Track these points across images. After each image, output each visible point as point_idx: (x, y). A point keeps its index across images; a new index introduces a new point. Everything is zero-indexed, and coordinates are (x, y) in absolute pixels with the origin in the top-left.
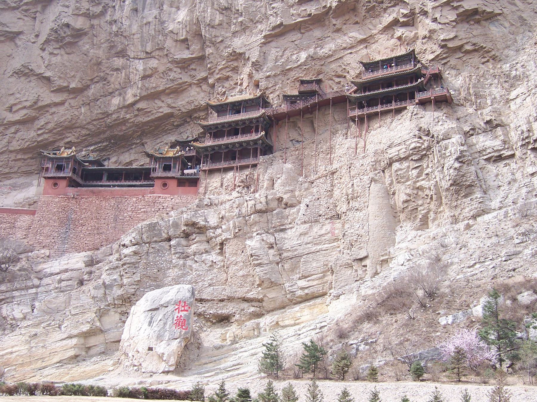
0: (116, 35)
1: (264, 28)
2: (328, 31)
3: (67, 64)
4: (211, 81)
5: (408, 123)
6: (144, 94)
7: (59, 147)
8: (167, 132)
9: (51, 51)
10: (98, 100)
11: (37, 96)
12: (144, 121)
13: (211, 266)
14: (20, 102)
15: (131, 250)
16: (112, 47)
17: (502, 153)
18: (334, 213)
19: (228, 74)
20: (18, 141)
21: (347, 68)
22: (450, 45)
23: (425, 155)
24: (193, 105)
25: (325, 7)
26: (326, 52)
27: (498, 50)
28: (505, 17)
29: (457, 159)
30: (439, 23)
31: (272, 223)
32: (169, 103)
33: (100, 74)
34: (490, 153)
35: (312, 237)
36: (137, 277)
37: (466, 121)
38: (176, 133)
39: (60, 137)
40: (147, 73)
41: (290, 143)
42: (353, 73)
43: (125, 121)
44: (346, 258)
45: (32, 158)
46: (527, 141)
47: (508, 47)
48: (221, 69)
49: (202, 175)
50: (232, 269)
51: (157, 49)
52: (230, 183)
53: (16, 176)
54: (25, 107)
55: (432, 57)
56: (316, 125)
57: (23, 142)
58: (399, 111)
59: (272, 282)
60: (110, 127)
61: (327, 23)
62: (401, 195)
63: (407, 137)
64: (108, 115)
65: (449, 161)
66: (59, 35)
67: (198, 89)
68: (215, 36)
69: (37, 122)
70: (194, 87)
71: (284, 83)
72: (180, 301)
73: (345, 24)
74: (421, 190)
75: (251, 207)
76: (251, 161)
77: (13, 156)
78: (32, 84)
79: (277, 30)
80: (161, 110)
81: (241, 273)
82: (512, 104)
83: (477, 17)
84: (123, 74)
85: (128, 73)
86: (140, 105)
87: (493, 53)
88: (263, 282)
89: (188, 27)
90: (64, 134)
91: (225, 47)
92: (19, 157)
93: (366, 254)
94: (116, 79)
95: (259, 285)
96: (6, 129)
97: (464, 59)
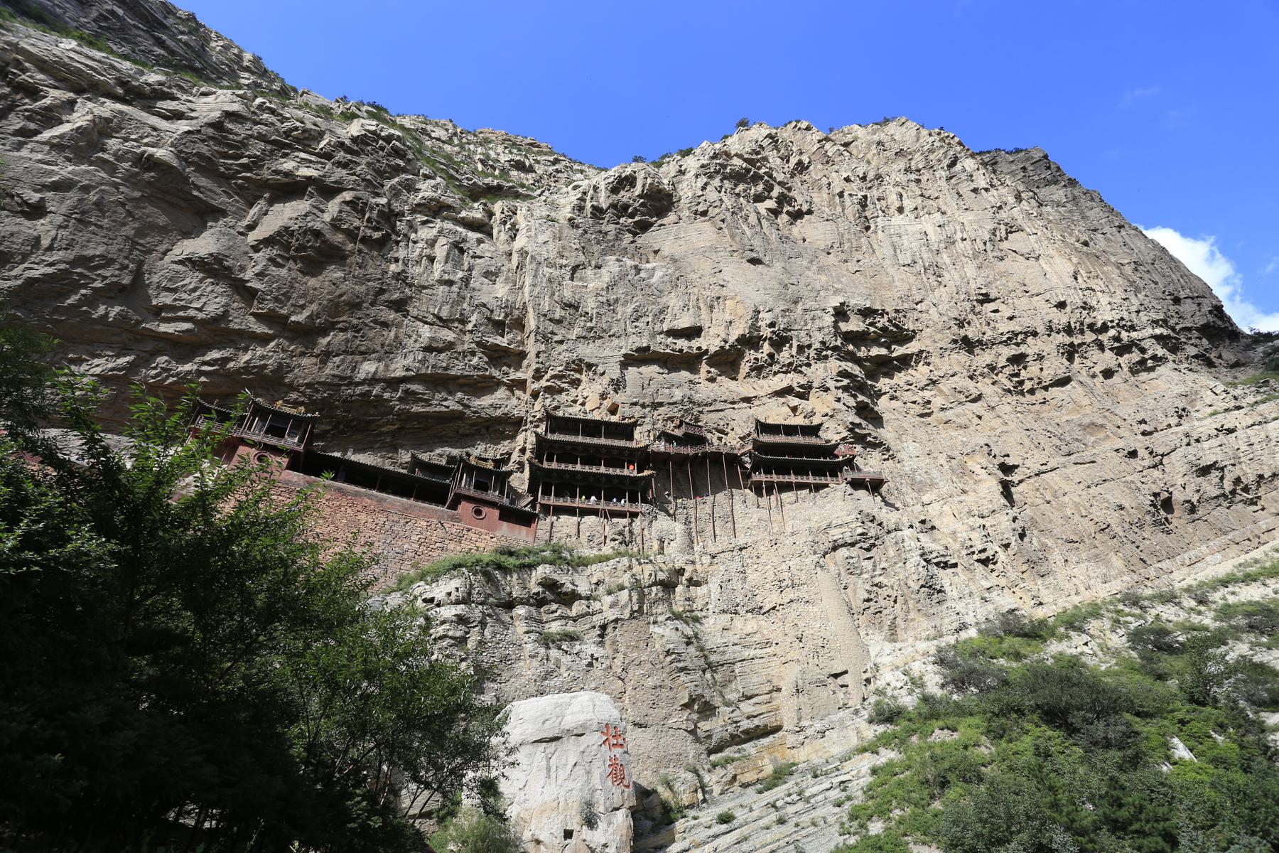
1: (629, 345)
5: (841, 503)
10: (338, 355)
13: (590, 665)
14: (185, 308)
15: (454, 612)
17: (947, 559)
19: (563, 385)
20: (155, 368)
21: (732, 423)
22: (857, 430)
25: (699, 348)
35: (738, 636)
40: (434, 345)
42: (741, 432)
44: (815, 673)
46: (972, 550)
48: (553, 377)
50: (634, 674)
52: (594, 533)
55: (838, 437)
56: (698, 483)
63: (848, 519)
64: (352, 383)
67: (508, 392)
68: (553, 333)
72: (607, 725)
74: (880, 587)
75: (651, 575)
78: (219, 289)
81: (650, 682)
84: (392, 334)
87: (891, 452)
95: (685, 706)
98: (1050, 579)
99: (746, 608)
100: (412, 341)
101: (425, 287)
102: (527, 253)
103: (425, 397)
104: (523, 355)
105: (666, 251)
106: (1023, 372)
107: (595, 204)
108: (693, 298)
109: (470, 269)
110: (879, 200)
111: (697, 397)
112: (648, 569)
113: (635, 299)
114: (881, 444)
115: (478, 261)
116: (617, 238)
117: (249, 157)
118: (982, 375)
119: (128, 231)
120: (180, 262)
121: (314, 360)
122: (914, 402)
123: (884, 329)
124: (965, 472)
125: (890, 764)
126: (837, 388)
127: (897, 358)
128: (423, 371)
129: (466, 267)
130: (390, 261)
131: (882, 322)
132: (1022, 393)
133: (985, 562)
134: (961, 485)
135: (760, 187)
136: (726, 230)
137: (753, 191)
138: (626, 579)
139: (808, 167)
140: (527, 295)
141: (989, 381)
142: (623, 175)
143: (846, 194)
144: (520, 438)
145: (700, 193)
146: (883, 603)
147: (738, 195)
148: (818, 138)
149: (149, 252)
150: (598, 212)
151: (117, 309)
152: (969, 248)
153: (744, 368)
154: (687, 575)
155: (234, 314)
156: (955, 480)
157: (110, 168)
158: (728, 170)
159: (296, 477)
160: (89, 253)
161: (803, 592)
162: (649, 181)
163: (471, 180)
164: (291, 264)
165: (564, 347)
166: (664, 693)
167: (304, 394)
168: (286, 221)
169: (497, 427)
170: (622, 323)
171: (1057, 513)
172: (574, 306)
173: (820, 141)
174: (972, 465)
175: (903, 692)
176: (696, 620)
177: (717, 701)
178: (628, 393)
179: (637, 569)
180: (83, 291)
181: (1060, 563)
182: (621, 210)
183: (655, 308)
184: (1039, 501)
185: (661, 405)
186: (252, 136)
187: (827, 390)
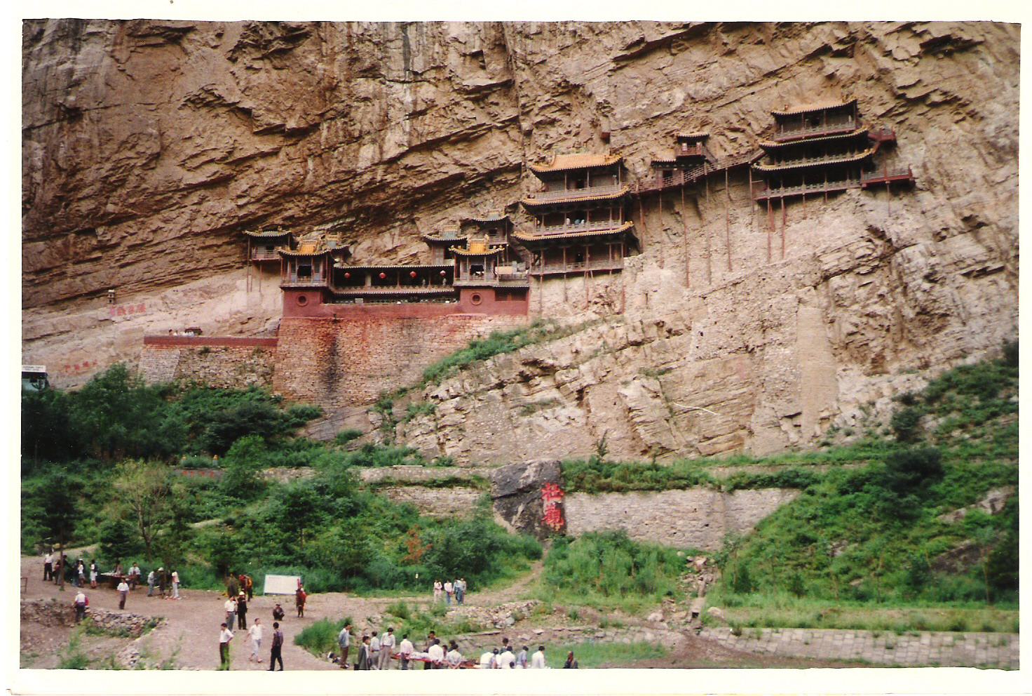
0: (361, 41)
2: (714, 52)
3: (279, 87)
4: (526, 125)
5: (850, 216)
6: (416, 142)
7: (272, 224)
8: (453, 203)
9: (249, 65)
10: (336, 149)
11: (232, 142)
12: (416, 186)
14: (203, 152)
16: (354, 61)
18: (741, 344)
21: (748, 117)
22: (911, 94)
23: (877, 267)
24: (496, 163)
26: (714, 89)
27: (979, 101)
28: (988, 48)
29: (928, 278)
30: (895, 59)
31: (653, 361)
32: (457, 157)
33: (336, 105)
34: (969, 266)
37: (935, 217)
38: (467, 204)
39: (275, 209)
40: (419, 109)
41: (664, 233)
42: (756, 127)
43: (383, 186)
45: (228, 243)
47: (992, 97)
48: (544, 108)
49: (533, 285)
51: (433, 68)
52: (580, 298)
53: (206, 273)
54: (212, 161)
55: (881, 111)
56: (701, 208)
57: (215, 219)
58: (833, 195)
59: (662, 448)
60: (361, 195)
61: (713, 38)
62: (843, 324)
63: (852, 239)
64: (356, 175)
65: (914, 280)
66: (262, 36)
67: (503, 137)
68: (532, 53)
69: (233, 184)
70: (497, 133)
71: (650, 138)
73: (741, 43)
76: (610, 265)
77: (200, 241)
78: (221, 121)
80: (443, 169)
81: (615, 435)
83: (949, 47)
84: (377, 107)
85: (384, 106)
86: (411, 160)
87: (971, 107)
88: (650, 447)
89: (483, 32)
90: (281, 204)
91: (549, 73)
92: (209, 242)
93: (799, 411)
94: (364, 117)
96: (185, 196)
97: (930, 115)
99: (729, 350)
103: (424, 169)
114: (956, 99)
146: (870, 335)
159: (328, 308)
160: (123, 137)
169: (499, 179)
178: (618, 116)
187: (874, 41)
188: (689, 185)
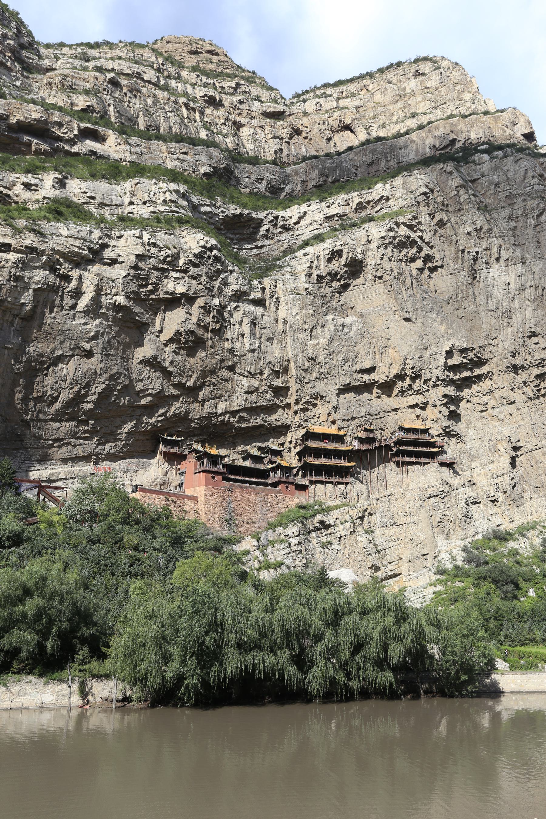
3: (186, 364)
5: (434, 474)
10: (208, 401)
14: (148, 389)
16: (223, 361)
21: (387, 425)
25: (374, 380)
36: (304, 561)
44: (417, 554)
45: (147, 440)
48: (305, 403)
50: (353, 556)
55: (437, 433)
63: (436, 483)
64: (216, 415)
76: (344, 480)
79: (347, 387)
80: (256, 421)
82: (474, 471)
84: (230, 385)
92: (141, 437)
95: (370, 568)
96: (134, 411)
98: (521, 508)
100: (239, 388)
101: (242, 356)
102: (287, 322)
104: (288, 388)
105: (358, 309)
106: (542, 383)
107: (319, 272)
108: (373, 345)
109: (260, 338)
110: (486, 250)
111: (372, 410)
112: (356, 511)
113: (343, 349)
114: (458, 434)
115: (264, 331)
116: (332, 299)
117: (152, 284)
118: (519, 388)
119: (120, 353)
120: (139, 363)
121: (198, 404)
122: (479, 404)
123: (471, 360)
124: (495, 450)
125: (440, 591)
126: (440, 405)
127: (475, 377)
128: (246, 406)
129: (258, 336)
130: (224, 341)
131: (471, 355)
132: (538, 398)
133: (493, 501)
134: (491, 458)
135: (414, 251)
136: (392, 293)
137: (410, 255)
138: (348, 518)
139: (446, 224)
140: (290, 353)
141: (520, 392)
142: (335, 249)
143: (466, 251)
144: (289, 435)
145: (379, 262)
147: (401, 261)
148: (456, 184)
149: (127, 362)
150: (320, 278)
151: (127, 398)
152: (533, 293)
153: (396, 391)
154: (368, 511)
155: (165, 387)
156: (490, 454)
157: (105, 316)
158: (397, 241)
161: (413, 519)
162: (351, 255)
163: (224, 212)
164: (182, 352)
165: (309, 385)
166: (363, 563)
167: (197, 423)
168: (177, 326)
170: (336, 367)
171: (535, 472)
172: (313, 359)
173: (457, 187)
174: (500, 447)
175: (448, 562)
176: (372, 532)
177: (380, 565)
179: (351, 512)
180: (115, 393)
181: (529, 499)
182: (333, 276)
183: (352, 355)
184: (527, 466)
185: (355, 418)
186: (150, 268)
187: (435, 406)
188: (372, 449)
